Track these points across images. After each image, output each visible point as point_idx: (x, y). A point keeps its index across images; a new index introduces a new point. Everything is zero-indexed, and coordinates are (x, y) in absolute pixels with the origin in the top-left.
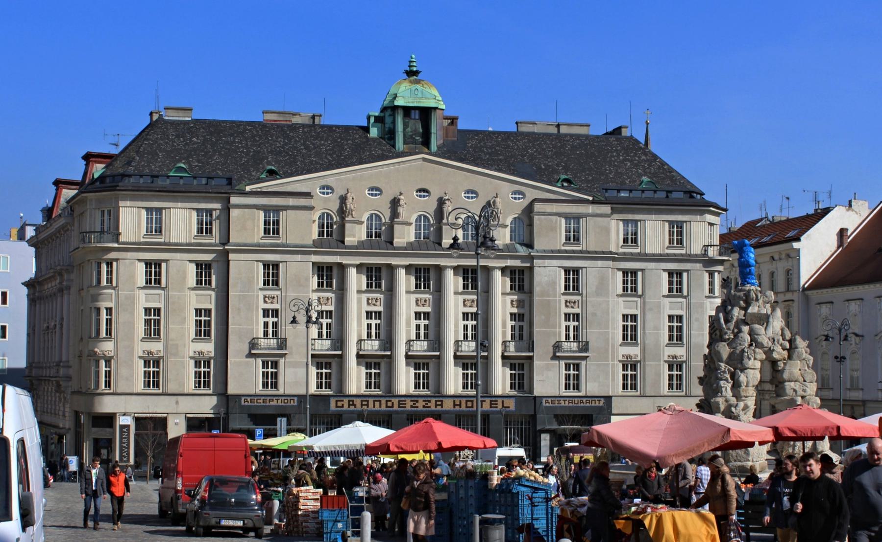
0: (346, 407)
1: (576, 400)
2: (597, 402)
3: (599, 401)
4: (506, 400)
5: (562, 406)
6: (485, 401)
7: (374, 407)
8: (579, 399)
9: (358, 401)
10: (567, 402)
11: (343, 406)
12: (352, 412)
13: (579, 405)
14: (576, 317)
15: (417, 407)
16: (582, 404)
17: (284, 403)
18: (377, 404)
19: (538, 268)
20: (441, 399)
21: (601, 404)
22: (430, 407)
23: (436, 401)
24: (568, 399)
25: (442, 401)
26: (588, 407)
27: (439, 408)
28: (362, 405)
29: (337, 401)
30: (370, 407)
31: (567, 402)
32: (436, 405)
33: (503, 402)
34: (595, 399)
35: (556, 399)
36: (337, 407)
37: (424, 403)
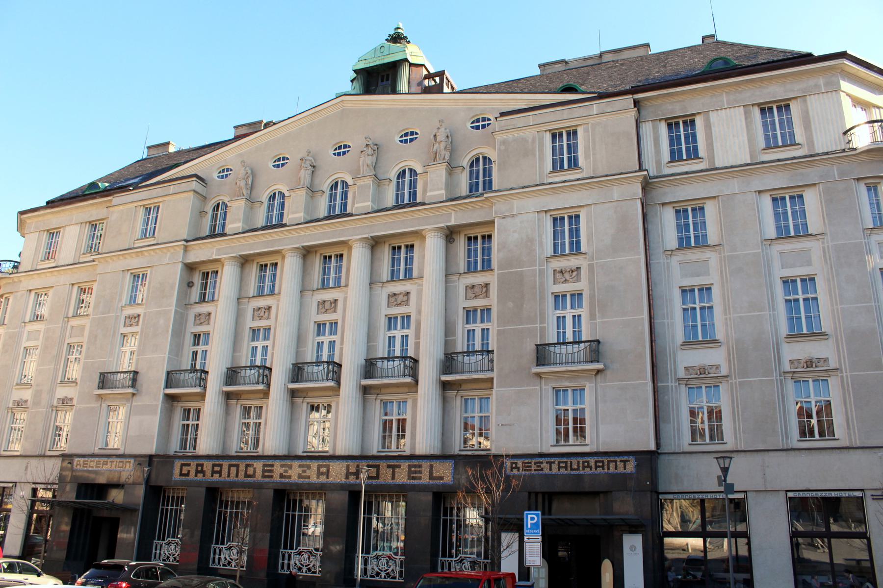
0: (192, 476)
1: (574, 461)
2: (620, 465)
3: (625, 462)
4: (436, 464)
5: (546, 475)
6: (399, 466)
7: (229, 476)
8: (581, 460)
9: (208, 465)
10: (555, 466)
11: (188, 475)
12: (199, 484)
13: (582, 472)
14: (577, 297)
15: (290, 477)
16: (587, 470)
17: (119, 467)
18: (234, 470)
19: (502, 221)
20: (326, 463)
21: (631, 467)
22: (309, 477)
23: (319, 467)
24: (557, 460)
25: (328, 467)
26: (599, 474)
27: (323, 479)
28: (213, 472)
29: (183, 465)
30: (223, 476)
31: (555, 466)
32: (319, 474)
33: (431, 467)
34: (616, 458)
35: (534, 461)
36: (181, 474)
37: (300, 470)
